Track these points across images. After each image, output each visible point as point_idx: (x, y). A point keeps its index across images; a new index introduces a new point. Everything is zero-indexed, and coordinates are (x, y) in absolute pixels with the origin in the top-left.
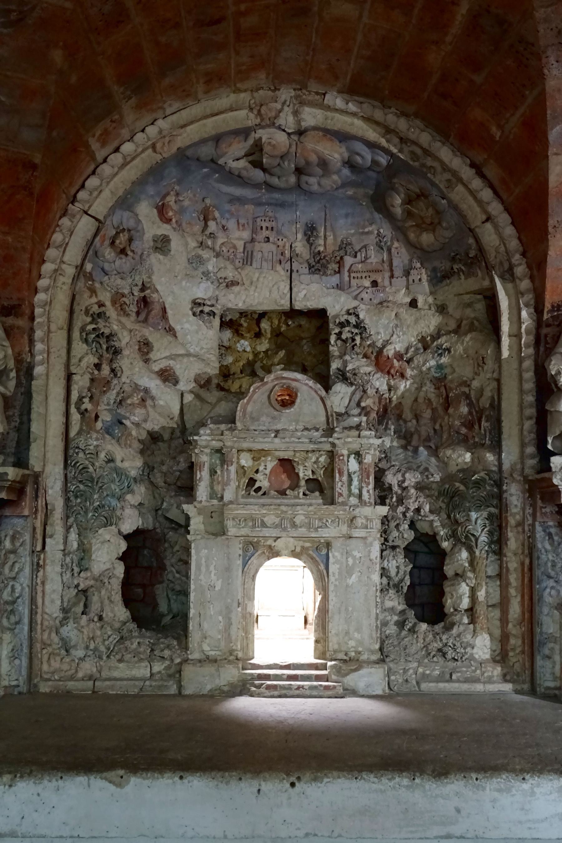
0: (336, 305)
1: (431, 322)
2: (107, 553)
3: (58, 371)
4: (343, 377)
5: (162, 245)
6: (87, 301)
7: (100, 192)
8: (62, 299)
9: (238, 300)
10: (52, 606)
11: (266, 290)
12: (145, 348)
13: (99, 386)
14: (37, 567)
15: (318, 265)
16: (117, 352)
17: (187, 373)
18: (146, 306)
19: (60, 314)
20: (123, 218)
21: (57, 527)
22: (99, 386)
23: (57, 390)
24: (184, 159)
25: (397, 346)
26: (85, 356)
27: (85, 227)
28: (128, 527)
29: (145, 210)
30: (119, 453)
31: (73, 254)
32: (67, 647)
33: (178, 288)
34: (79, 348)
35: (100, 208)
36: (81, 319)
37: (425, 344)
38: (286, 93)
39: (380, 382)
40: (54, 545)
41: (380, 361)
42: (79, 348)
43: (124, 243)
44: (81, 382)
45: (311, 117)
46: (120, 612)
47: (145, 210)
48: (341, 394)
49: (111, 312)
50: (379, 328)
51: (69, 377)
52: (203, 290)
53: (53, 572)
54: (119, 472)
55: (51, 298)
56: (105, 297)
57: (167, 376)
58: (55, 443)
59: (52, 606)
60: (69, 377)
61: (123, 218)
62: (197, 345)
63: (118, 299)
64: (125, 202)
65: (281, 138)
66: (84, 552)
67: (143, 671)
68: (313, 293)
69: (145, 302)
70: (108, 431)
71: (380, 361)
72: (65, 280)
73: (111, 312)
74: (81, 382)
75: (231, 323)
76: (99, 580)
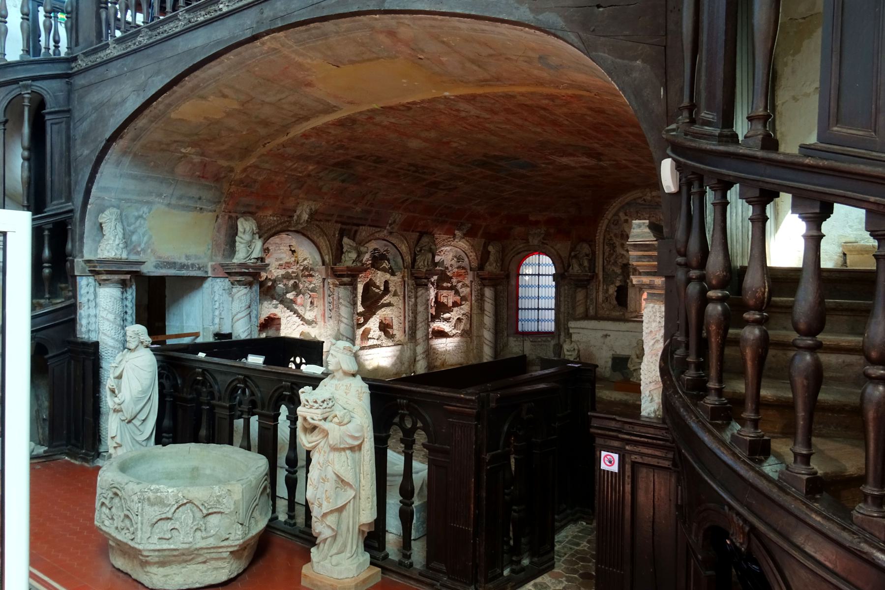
2: (612, 290)
3: (601, 252)
6: (608, 237)
7: (609, 215)
8: (602, 237)
10: (600, 300)
13: (611, 255)
14: (597, 292)
16: (615, 247)
19: (601, 240)
20: (616, 218)
21: (601, 285)
22: (611, 255)
23: (601, 256)
24: (627, 204)
26: (607, 248)
27: (606, 221)
28: (618, 284)
29: (621, 214)
30: (615, 269)
31: (604, 228)
32: (603, 308)
34: (606, 247)
35: (609, 217)
36: (606, 241)
38: (648, 190)
40: (601, 288)
42: (606, 247)
43: (616, 223)
44: (607, 254)
46: (615, 302)
47: (621, 214)
49: (614, 238)
51: (604, 254)
53: (600, 293)
54: (616, 273)
55: (600, 237)
56: (612, 235)
58: (601, 268)
59: (600, 300)
60: (604, 254)
61: (616, 218)
63: (616, 235)
64: (616, 214)
65: (649, 198)
66: (607, 290)
67: (618, 314)
69: (622, 235)
70: (613, 264)
72: (602, 233)
73: (614, 238)
74: (607, 254)
76: (610, 295)
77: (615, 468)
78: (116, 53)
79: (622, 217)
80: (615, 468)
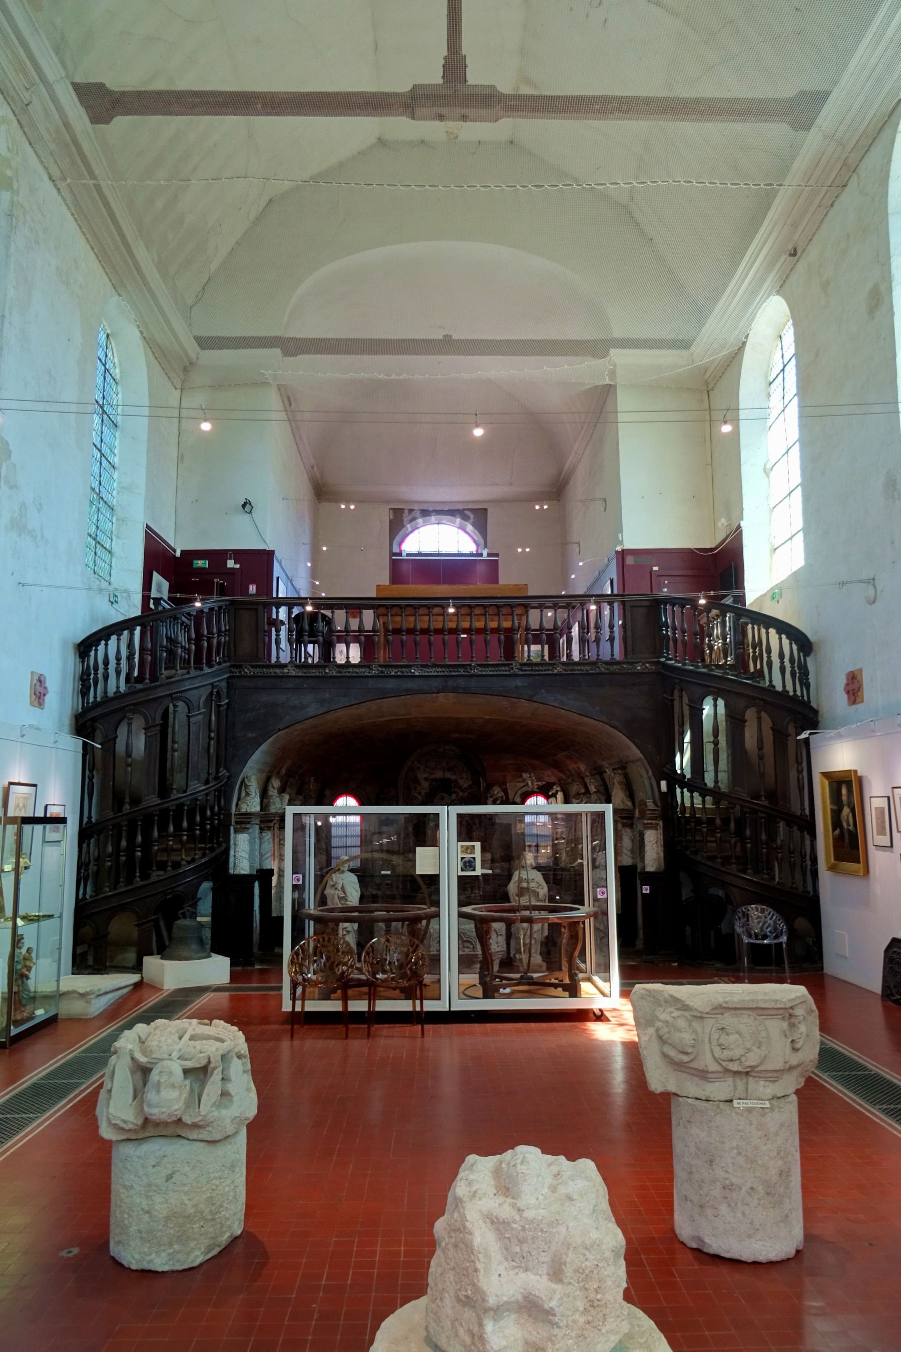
0: (453, 777)
1: (471, 782)
4: (454, 792)
5: (419, 768)
9: (433, 776)
11: (439, 775)
12: (416, 788)
15: (450, 769)
17: (423, 792)
18: (416, 781)
25: (465, 786)
33: (421, 776)
37: (470, 786)
39: (461, 794)
41: (462, 790)
45: (447, 747)
48: (454, 796)
50: (461, 782)
52: (426, 775)
57: (420, 793)
62: (426, 785)
68: (448, 775)
71: (460, 788)
75: (433, 780)
77: (648, 892)
78: (293, 673)
79: (417, 765)
80: (648, 892)
